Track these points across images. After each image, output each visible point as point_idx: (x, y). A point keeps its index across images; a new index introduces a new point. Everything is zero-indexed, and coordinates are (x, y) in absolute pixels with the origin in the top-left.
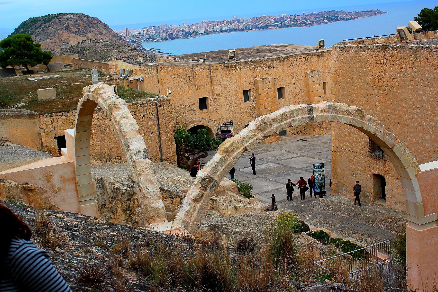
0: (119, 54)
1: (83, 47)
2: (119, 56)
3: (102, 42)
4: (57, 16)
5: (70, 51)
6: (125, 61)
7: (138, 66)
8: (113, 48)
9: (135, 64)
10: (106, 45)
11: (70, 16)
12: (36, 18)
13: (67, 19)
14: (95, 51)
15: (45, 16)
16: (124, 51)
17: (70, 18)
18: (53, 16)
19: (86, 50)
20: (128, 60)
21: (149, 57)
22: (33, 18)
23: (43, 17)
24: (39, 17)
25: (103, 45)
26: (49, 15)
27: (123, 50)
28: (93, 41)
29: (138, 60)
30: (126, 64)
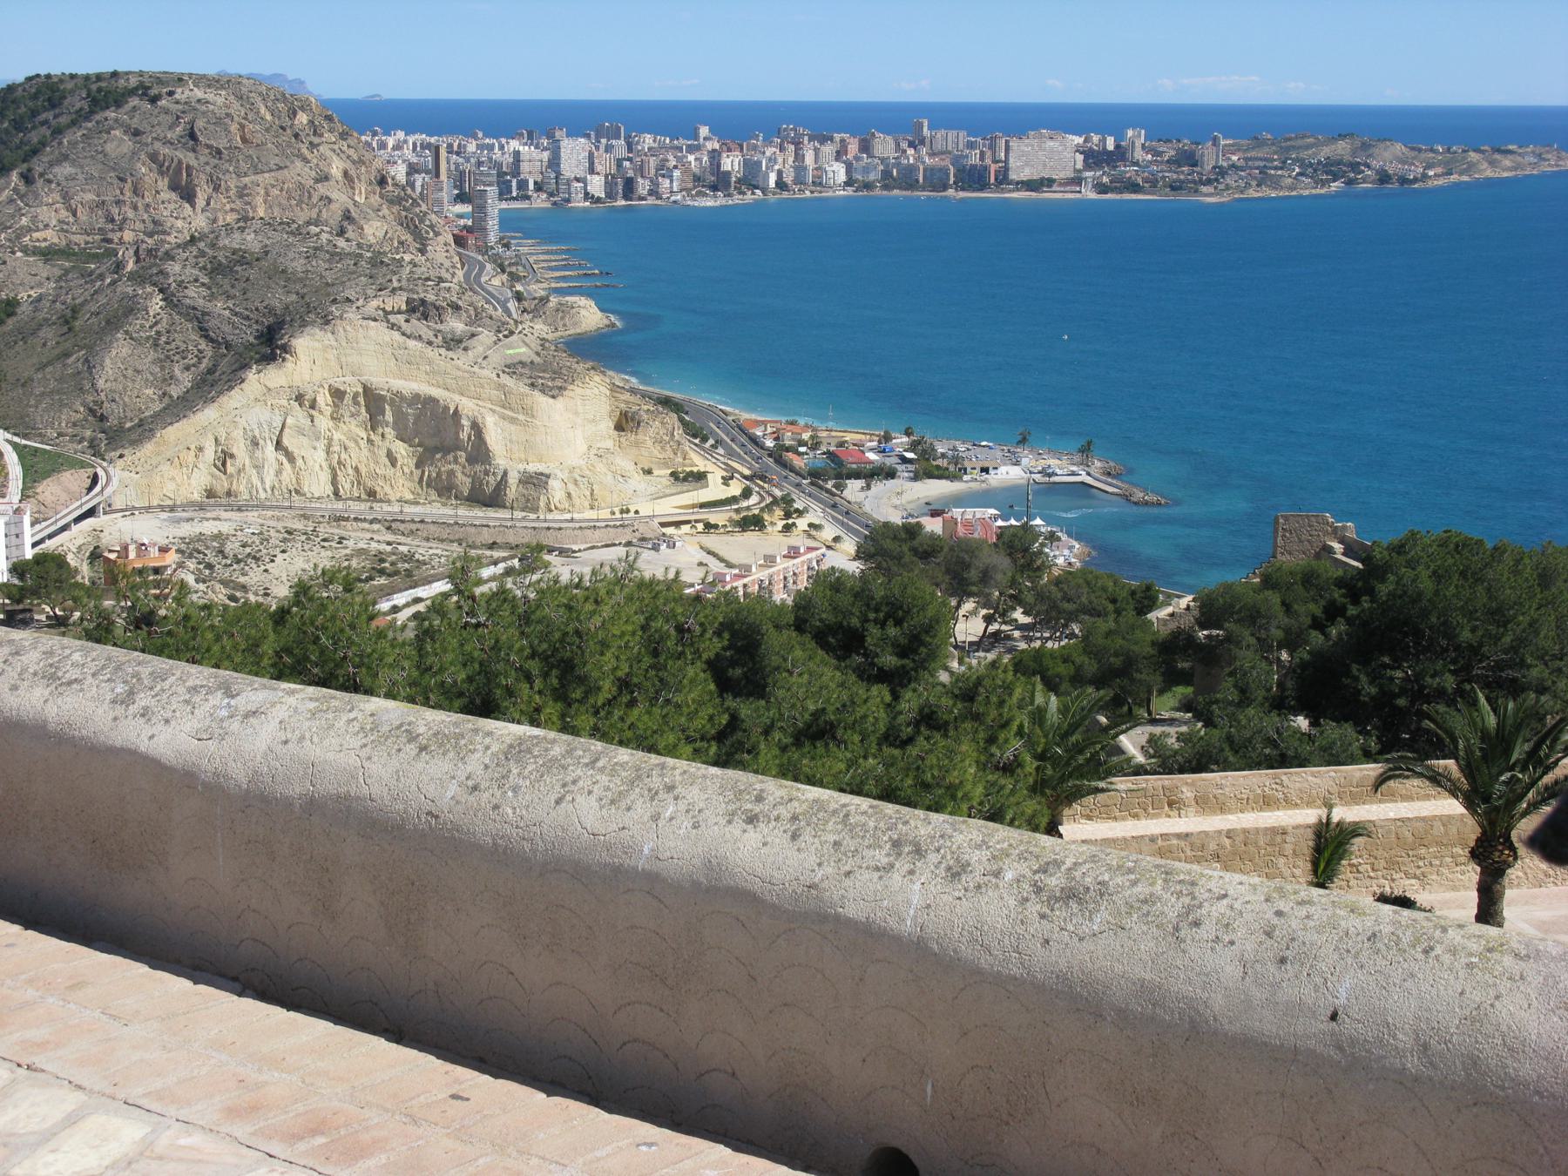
0: (375, 296)
1: (237, 247)
2: (375, 303)
3: (317, 235)
4: (149, 89)
5: (187, 260)
6: (393, 326)
7: (443, 351)
8: (355, 264)
9: (430, 343)
10: (329, 248)
11: (199, 93)
12: (62, 79)
13: (186, 103)
14: (283, 271)
15: (99, 77)
16: (396, 284)
17: (199, 101)
18: (133, 82)
19: (247, 263)
20: (404, 326)
21: (491, 318)
22: (48, 76)
23: (87, 78)
24: (72, 76)
25: (316, 249)
26: (115, 74)
27: (390, 281)
28: (279, 228)
29: (439, 327)
30: (396, 335)
